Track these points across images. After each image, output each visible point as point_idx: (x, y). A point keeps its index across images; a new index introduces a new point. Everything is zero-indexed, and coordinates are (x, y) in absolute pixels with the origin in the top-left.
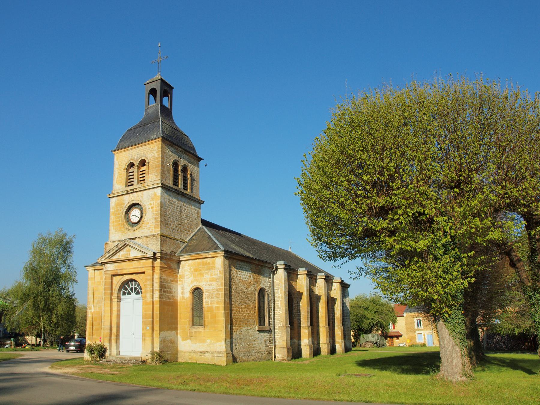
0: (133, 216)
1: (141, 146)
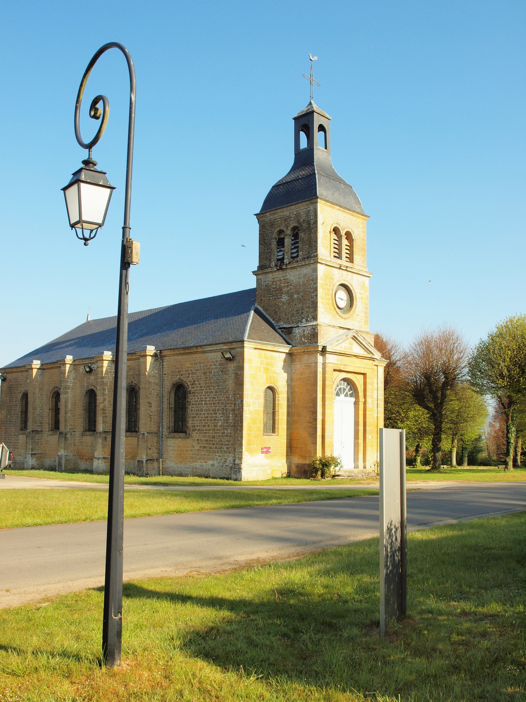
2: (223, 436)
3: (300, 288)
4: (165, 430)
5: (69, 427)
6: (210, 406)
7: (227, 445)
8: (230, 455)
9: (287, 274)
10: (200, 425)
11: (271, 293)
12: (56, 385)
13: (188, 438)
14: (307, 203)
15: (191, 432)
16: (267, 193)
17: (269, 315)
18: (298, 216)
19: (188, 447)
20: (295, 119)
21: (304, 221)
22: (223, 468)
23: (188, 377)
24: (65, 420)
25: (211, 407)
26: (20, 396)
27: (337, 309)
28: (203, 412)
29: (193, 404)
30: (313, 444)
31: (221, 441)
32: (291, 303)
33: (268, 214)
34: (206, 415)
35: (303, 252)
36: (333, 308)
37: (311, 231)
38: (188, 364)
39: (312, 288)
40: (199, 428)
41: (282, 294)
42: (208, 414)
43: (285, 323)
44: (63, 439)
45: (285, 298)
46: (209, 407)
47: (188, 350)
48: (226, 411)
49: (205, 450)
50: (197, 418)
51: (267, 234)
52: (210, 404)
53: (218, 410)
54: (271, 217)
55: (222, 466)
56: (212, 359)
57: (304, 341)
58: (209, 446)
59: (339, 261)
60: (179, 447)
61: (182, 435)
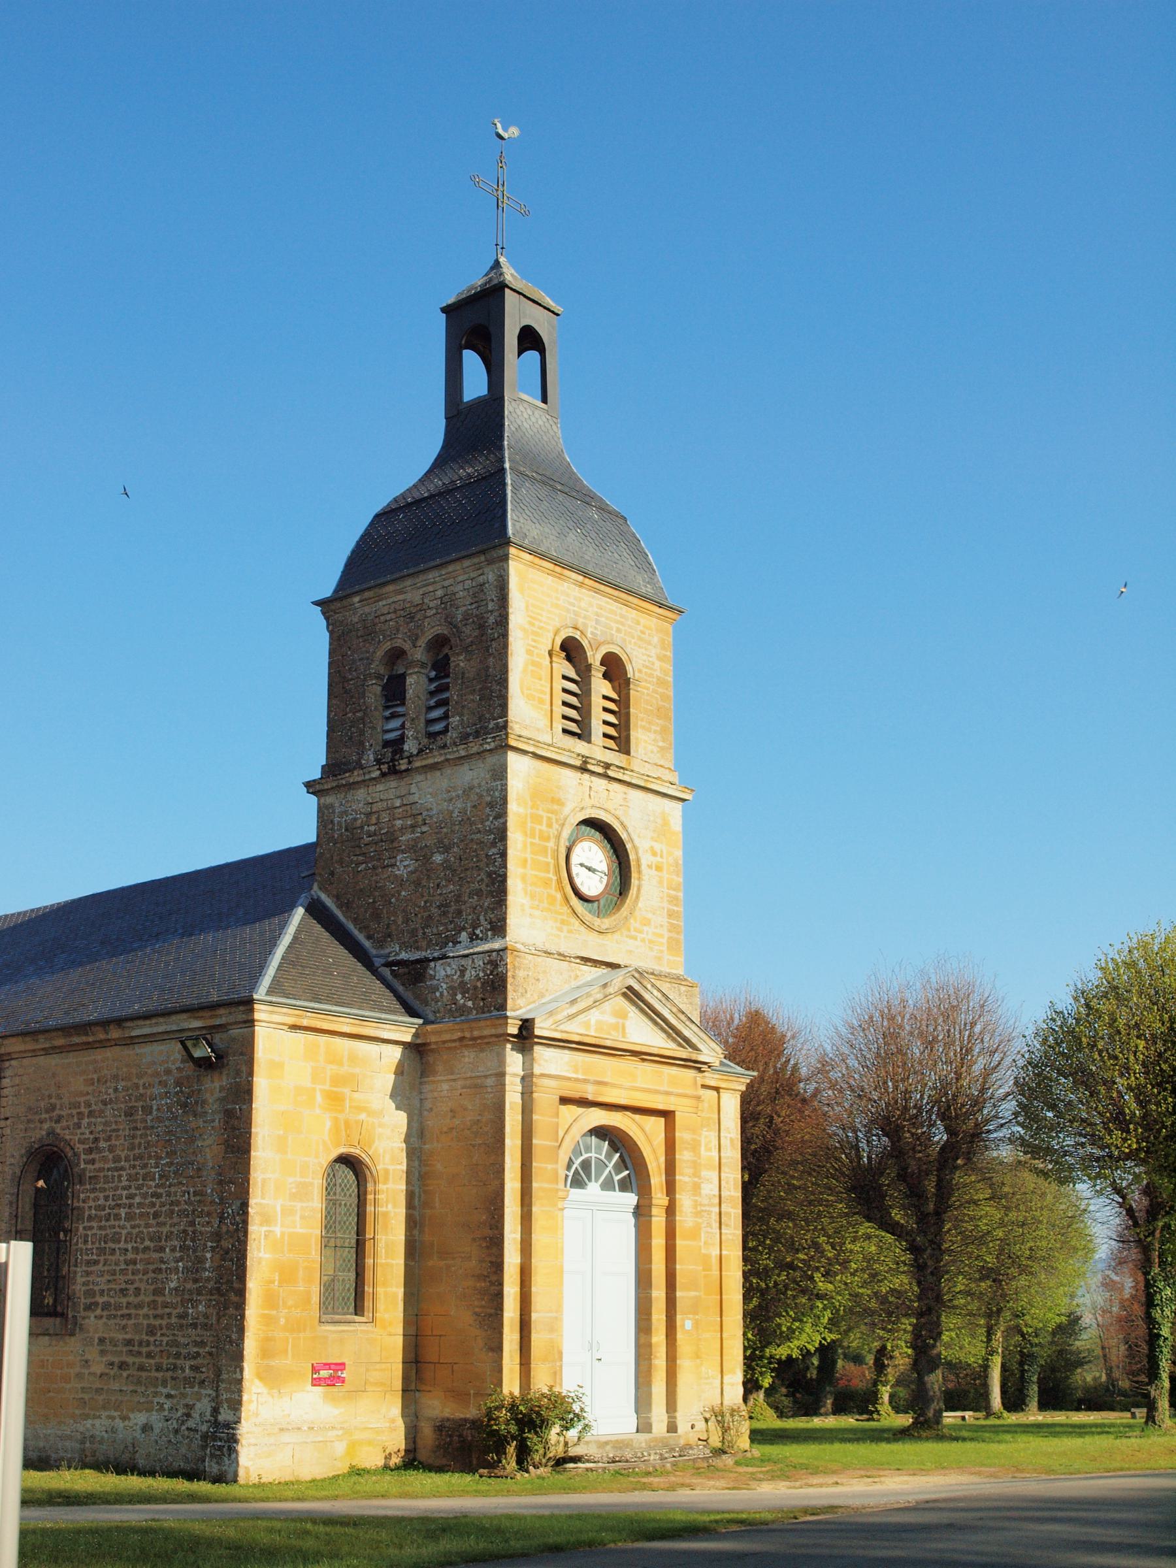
0: (582, 865)
1: (610, 597)
6: (142, 1223)
7: (194, 1358)
8: (204, 1392)
9: (414, 789)
10: (110, 1290)
13: (72, 1334)
14: (476, 560)
15: (83, 1314)
17: (355, 921)
18: (449, 601)
19: (70, 1365)
21: (466, 618)
23: (78, 1126)
25: (147, 1226)
27: (574, 901)
28: (122, 1245)
29: (90, 1218)
31: (175, 1343)
32: (424, 883)
33: (356, 599)
34: (130, 1256)
35: (461, 715)
36: (559, 896)
39: (490, 832)
40: (105, 1299)
41: (394, 851)
43: (405, 946)
45: (404, 866)
46: (139, 1226)
47: (78, 1035)
48: (193, 1240)
49: (125, 1374)
50: (100, 1267)
51: (354, 661)
52: (142, 1215)
54: (367, 609)
55: (176, 1431)
56: (154, 1063)
57: (464, 1005)
58: (137, 1360)
59: (580, 747)
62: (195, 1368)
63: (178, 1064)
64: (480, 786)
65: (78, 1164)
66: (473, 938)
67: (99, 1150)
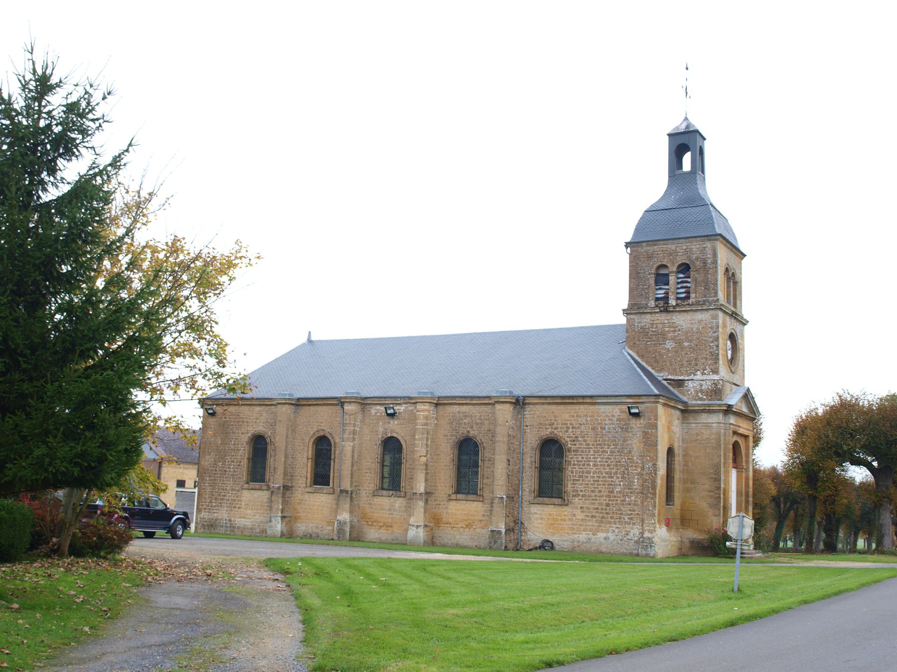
2: (623, 505)
3: (693, 335)
4: (526, 493)
5: (354, 484)
6: (602, 468)
7: (629, 515)
9: (674, 317)
11: (650, 337)
12: (322, 428)
13: (567, 505)
14: (703, 239)
16: (639, 218)
17: (647, 363)
18: (688, 252)
19: (565, 515)
20: (669, 135)
21: (697, 259)
22: (623, 542)
23: (567, 431)
24: (352, 475)
26: (245, 438)
28: (591, 475)
29: (574, 465)
30: (716, 516)
31: (621, 510)
32: (680, 352)
33: (645, 244)
34: (595, 479)
37: (707, 271)
38: (566, 416)
39: (711, 337)
40: (584, 493)
41: (665, 339)
42: (599, 477)
43: (671, 374)
44: (348, 499)
45: (670, 345)
48: (628, 475)
49: (594, 520)
50: (580, 482)
51: (642, 267)
52: (601, 465)
53: (616, 473)
54: (648, 248)
55: (622, 540)
56: (605, 412)
57: (702, 398)
58: (601, 515)
60: (550, 515)
61: (557, 501)
62: (631, 519)
63: (618, 414)
64: (706, 320)
65: (567, 445)
66: (703, 374)
67: (578, 441)
